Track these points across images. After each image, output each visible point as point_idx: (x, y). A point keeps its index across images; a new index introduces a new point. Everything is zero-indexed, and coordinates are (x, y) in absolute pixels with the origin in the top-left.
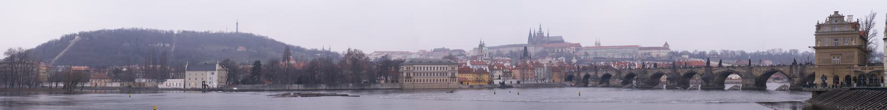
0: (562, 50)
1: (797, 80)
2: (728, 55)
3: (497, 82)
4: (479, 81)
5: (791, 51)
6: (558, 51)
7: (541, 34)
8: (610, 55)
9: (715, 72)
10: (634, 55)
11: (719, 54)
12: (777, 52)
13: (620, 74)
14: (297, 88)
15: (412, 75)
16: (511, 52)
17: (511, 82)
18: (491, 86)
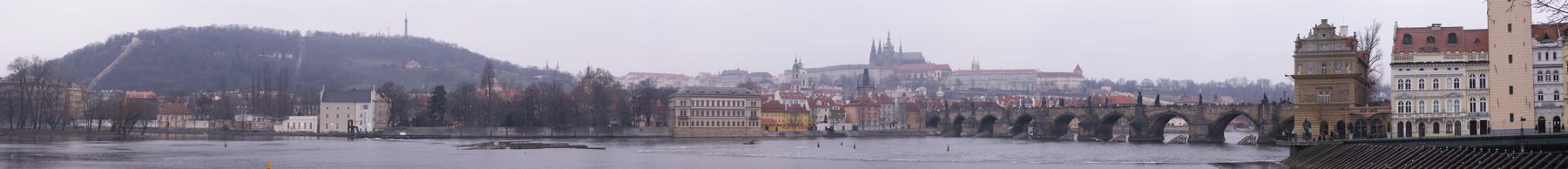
0: (922, 76)
1: (1268, 128)
2: (1168, 87)
3: (821, 127)
4: (792, 125)
5: (1260, 81)
6: (916, 76)
7: (889, 47)
8: (993, 85)
9: (1149, 114)
10: (1030, 86)
11: (1156, 85)
12: (1239, 82)
13: (1008, 116)
14: (505, 134)
15: (688, 114)
16: (843, 77)
17: (843, 127)
18: (812, 133)
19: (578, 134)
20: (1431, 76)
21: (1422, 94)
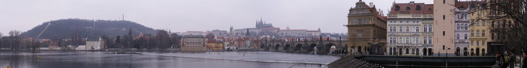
3: (226, 48)
4: (217, 47)
7: (262, 22)
8: (293, 35)
9: (324, 44)
11: (345, 35)
13: (283, 45)
17: (233, 48)
18: (224, 50)
19: (153, 50)
20: (406, 25)
21: (401, 34)
